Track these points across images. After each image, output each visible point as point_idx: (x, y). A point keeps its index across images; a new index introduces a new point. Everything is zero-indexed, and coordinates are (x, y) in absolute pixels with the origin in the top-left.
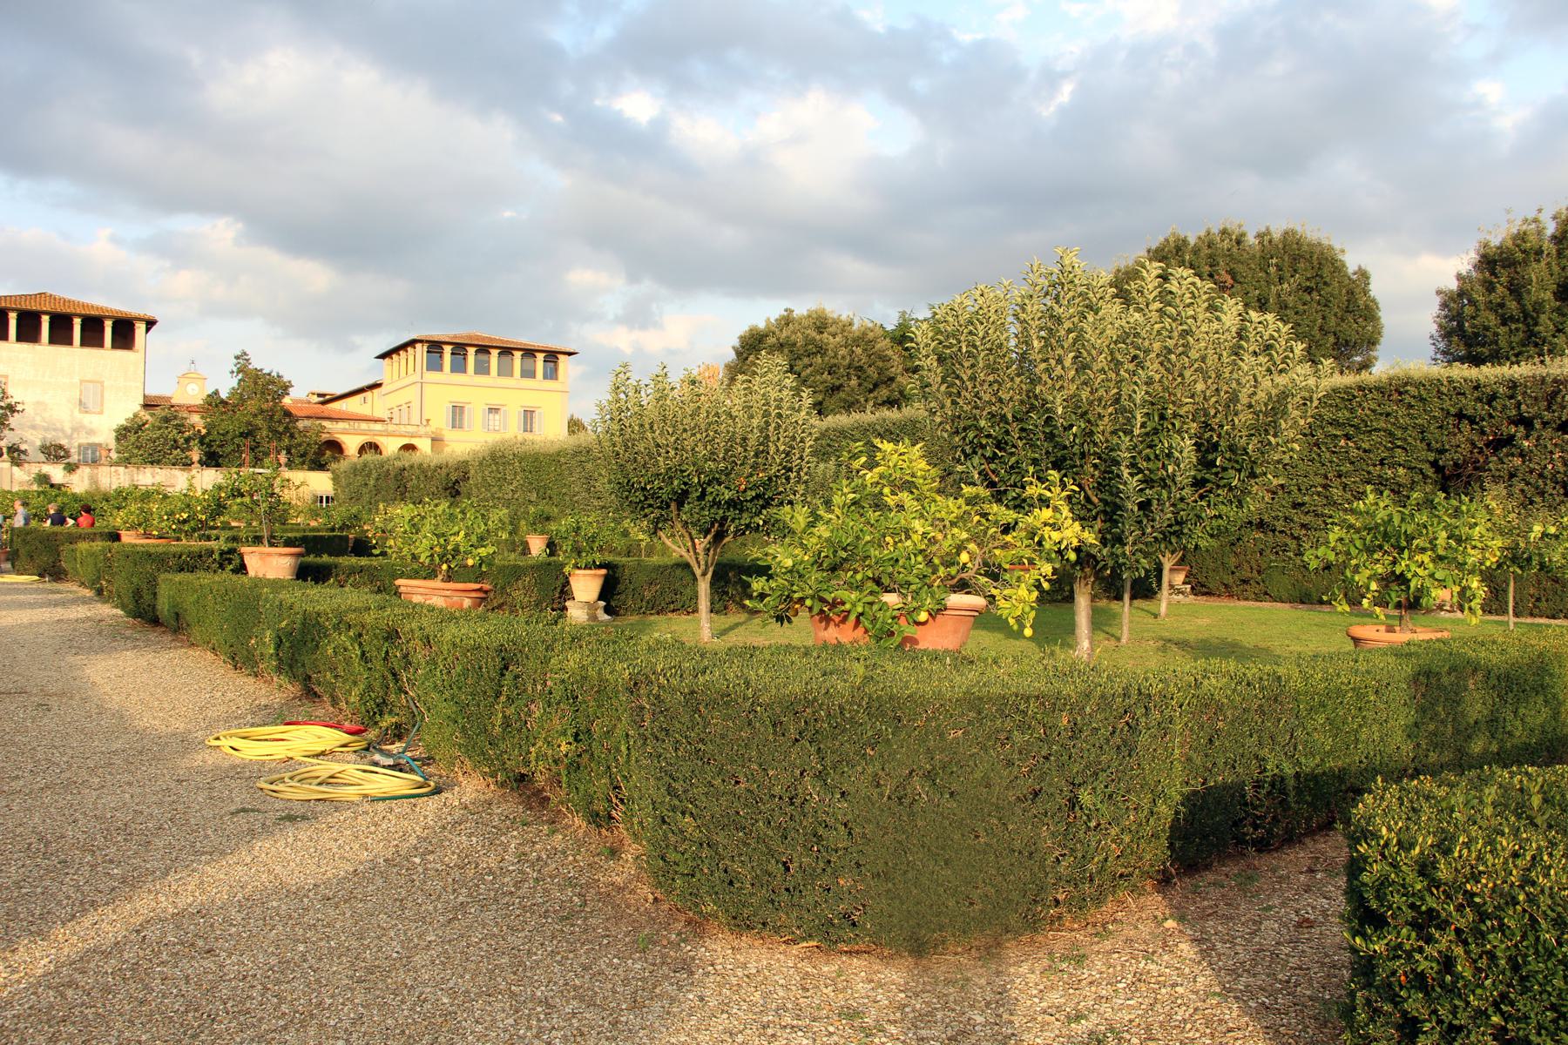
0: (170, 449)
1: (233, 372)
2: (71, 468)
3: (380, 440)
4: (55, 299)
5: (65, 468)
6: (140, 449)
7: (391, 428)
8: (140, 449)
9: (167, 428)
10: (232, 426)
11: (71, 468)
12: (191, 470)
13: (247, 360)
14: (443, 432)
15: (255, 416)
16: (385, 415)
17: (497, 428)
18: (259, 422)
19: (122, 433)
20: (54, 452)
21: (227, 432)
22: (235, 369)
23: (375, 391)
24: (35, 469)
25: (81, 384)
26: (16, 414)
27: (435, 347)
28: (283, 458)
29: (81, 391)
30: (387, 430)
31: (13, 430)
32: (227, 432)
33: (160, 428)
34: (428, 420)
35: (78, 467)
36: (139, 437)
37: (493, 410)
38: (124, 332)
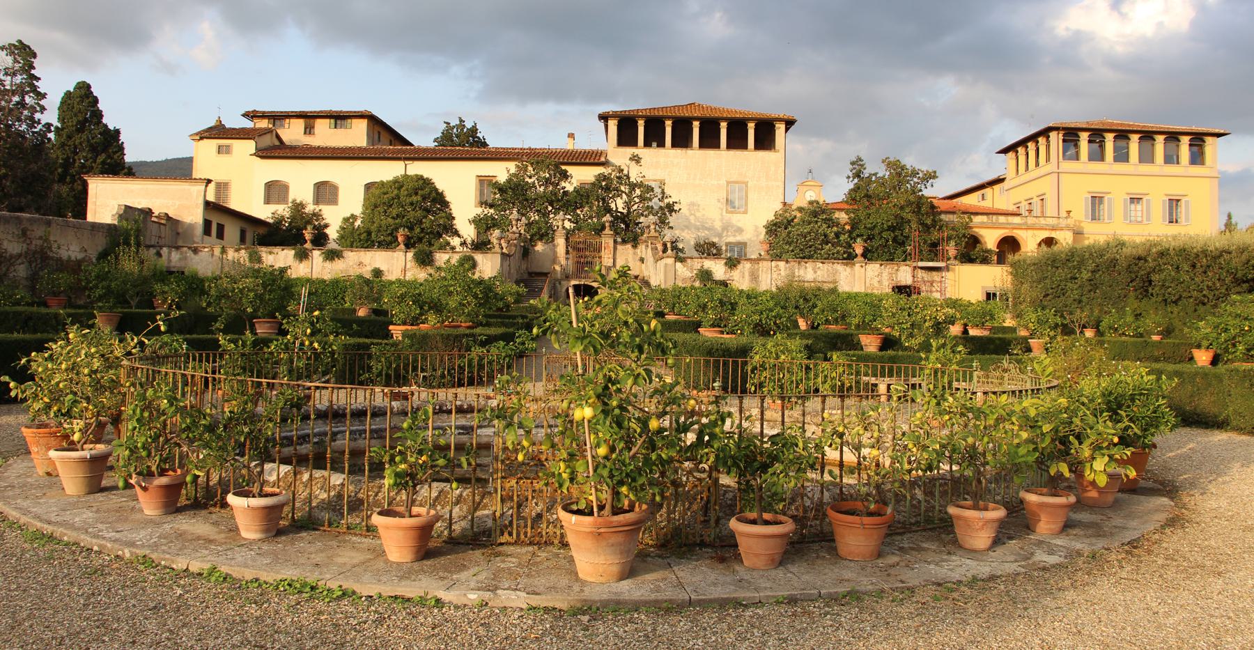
0: (821, 244)
1: (848, 177)
2: (732, 264)
3: (1020, 235)
4: (703, 107)
5: (726, 264)
6: (790, 245)
7: (1030, 221)
8: (790, 245)
9: (817, 222)
10: (882, 216)
11: (732, 264)
12: (854, 264)
13: (862, 165)
14: (1082, 225)
15: (902, 208)
16: (1012, 208)
17: (1139, 219)
18: (907, 214)
19: (773, 229)
20: (708, 249)
21: (875, 226)
22: (851, 174)
23: (996, 187)
24: (697, 264)
25: (727, 185)
26: (673, 213)
27: (1071, 135)
28: (952, 250)
29: (727, 191)
30: (1026, 223)
31: (672, 228)
32: (875, 226)
33: (810, 223)
34: (1069, 212)
35: (739, 262)
36: (789, 233)
37: (1135, 200)
38: (765, 139)
